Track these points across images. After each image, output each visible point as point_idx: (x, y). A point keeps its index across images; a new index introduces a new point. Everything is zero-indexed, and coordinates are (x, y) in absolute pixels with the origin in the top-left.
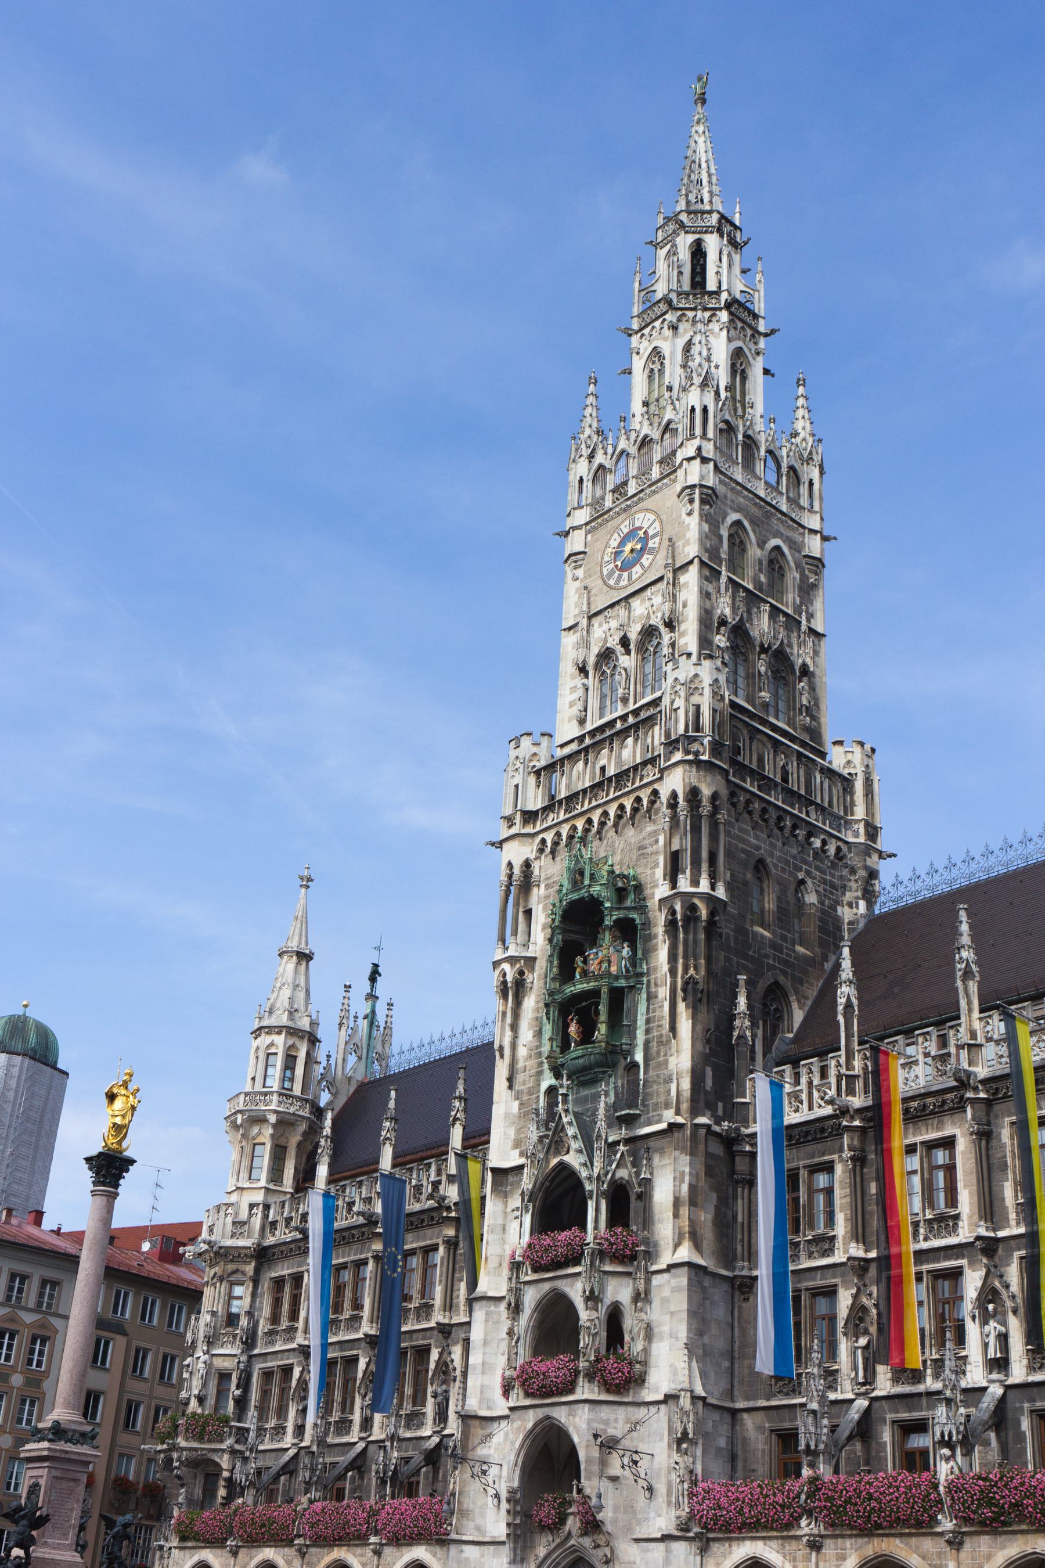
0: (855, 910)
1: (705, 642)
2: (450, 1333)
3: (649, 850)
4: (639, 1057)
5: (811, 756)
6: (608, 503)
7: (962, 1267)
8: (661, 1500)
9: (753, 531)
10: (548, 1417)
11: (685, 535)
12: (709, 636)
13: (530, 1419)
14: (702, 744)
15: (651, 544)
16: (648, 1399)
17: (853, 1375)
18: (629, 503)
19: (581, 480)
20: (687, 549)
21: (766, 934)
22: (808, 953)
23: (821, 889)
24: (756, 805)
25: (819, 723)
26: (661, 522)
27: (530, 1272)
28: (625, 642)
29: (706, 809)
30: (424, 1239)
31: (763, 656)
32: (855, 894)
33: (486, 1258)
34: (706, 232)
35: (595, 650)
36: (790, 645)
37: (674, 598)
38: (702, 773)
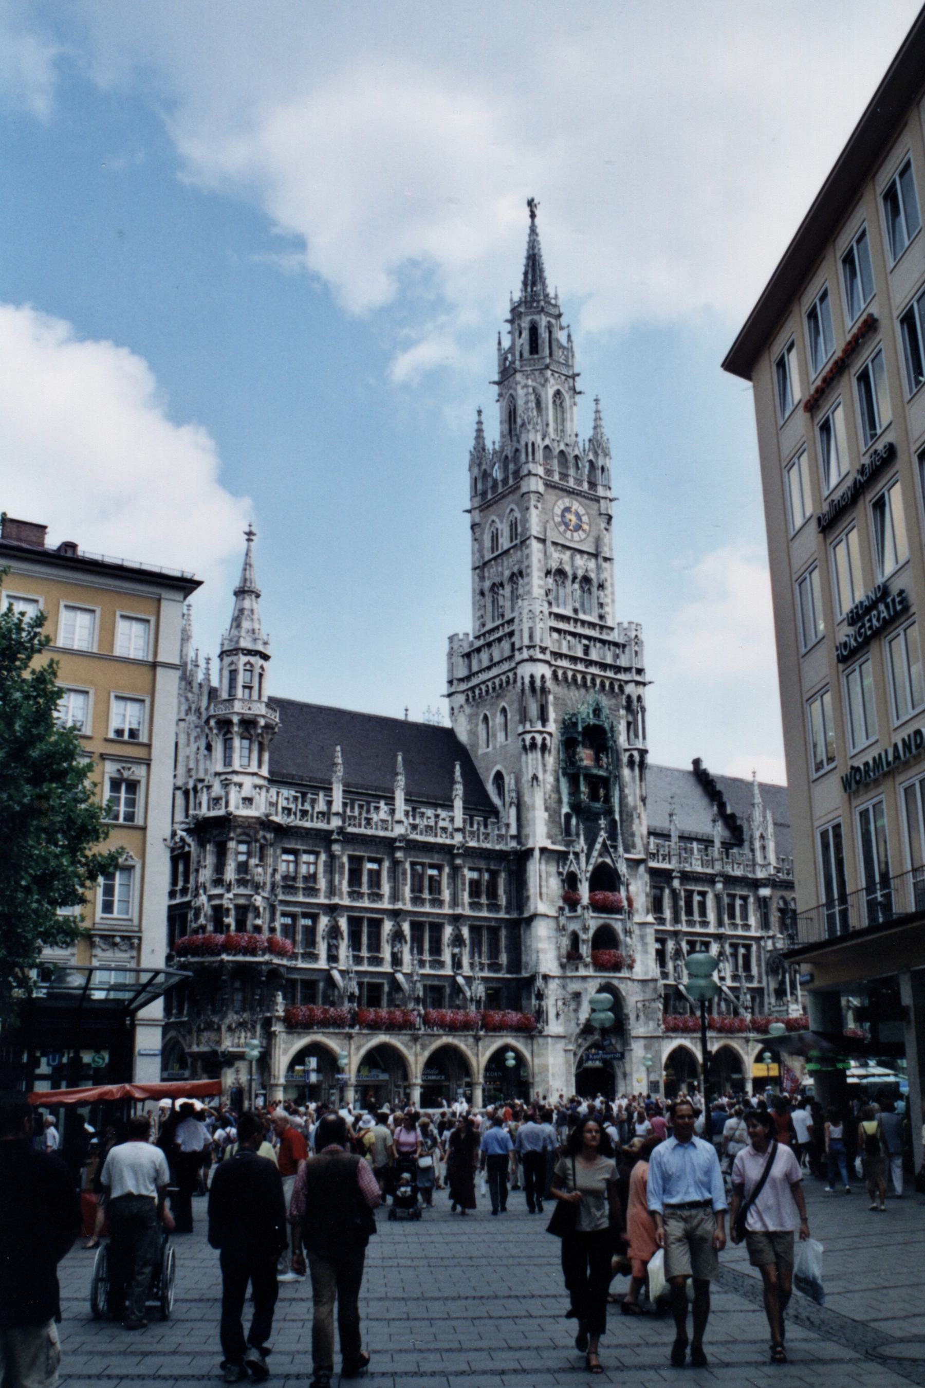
4: (617, 817)
30: (432, 858)
33: (541, 894)
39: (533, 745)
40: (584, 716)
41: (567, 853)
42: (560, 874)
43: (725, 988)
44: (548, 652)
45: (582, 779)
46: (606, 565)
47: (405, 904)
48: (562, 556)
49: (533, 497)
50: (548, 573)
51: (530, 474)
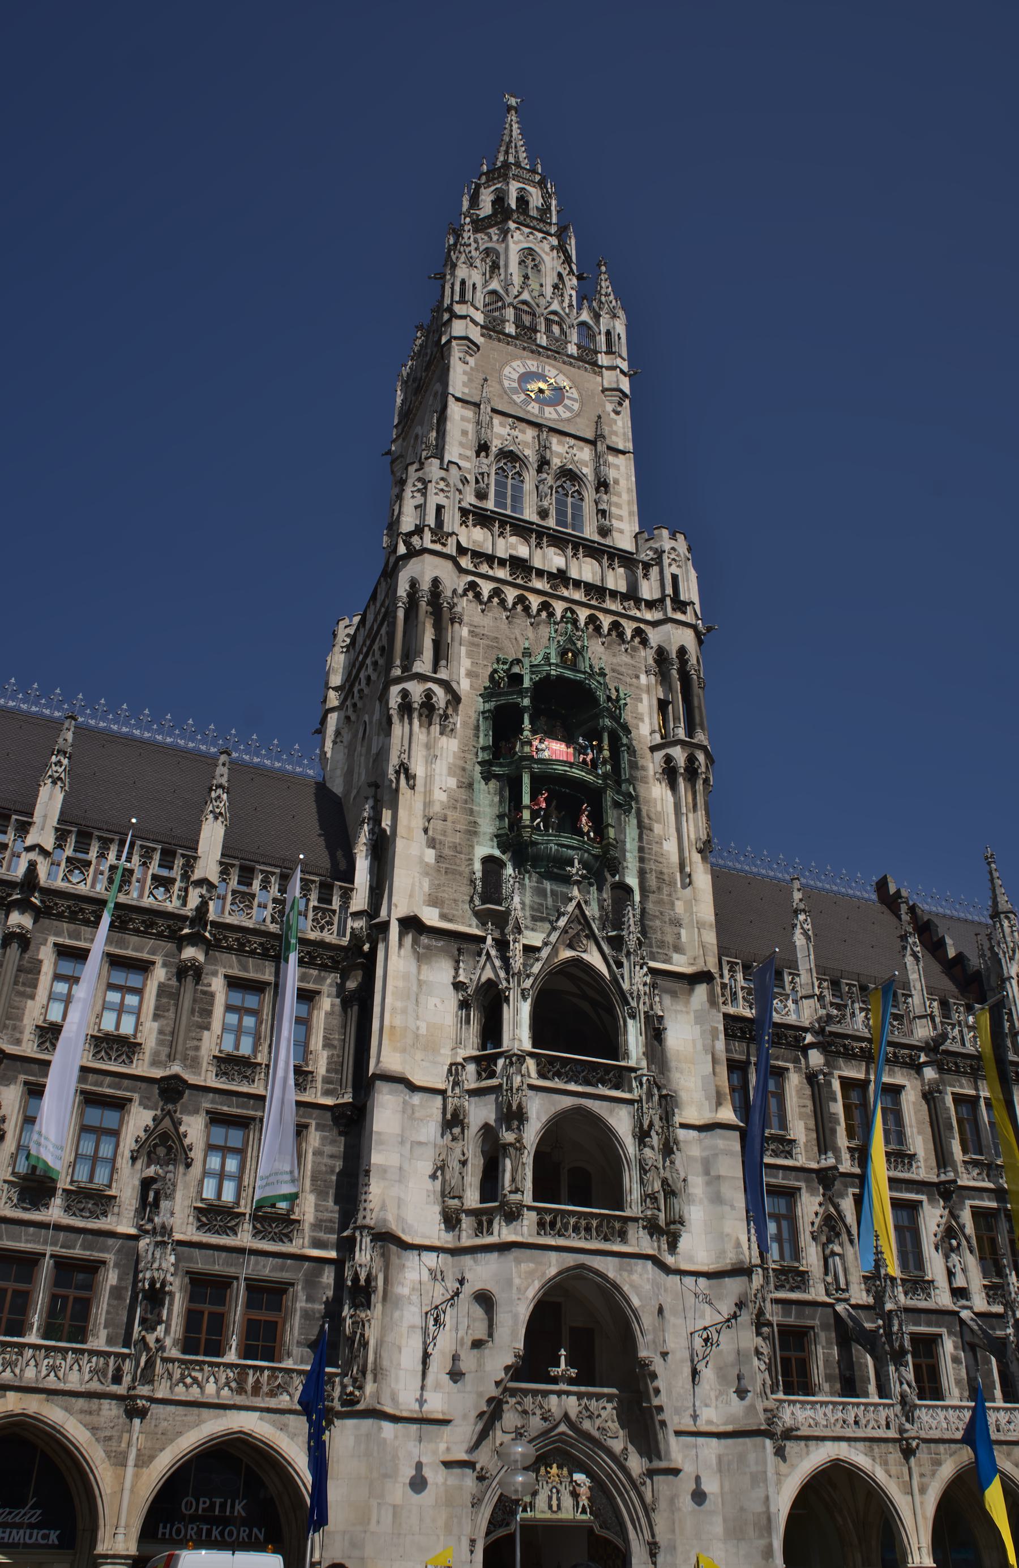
2: (181, 1094)
3: (628, 680)
4: (632, 881)
7: (921, 1202)
8: (707, 1387)
10: (582, 1266)
11: (611, 426)
13: (553, 1265)
15: (567, 401)
16: (684, 1266)
17: (829, 1279)
19: (474, 285)
20: (614, 438)
26: (580, 393)
27: (534, 1073)
39: (406, 708)
40: (538, 659)
41: (483, 940)
42: (458, 986)
43: (965, 1314)
44: (452, 542)
45: (526, 780)
46: (620, 461)
47: (18, 1042)
48: (516, 433)
49: (457, 351)
50: (483, 448)
51: (454, 316)
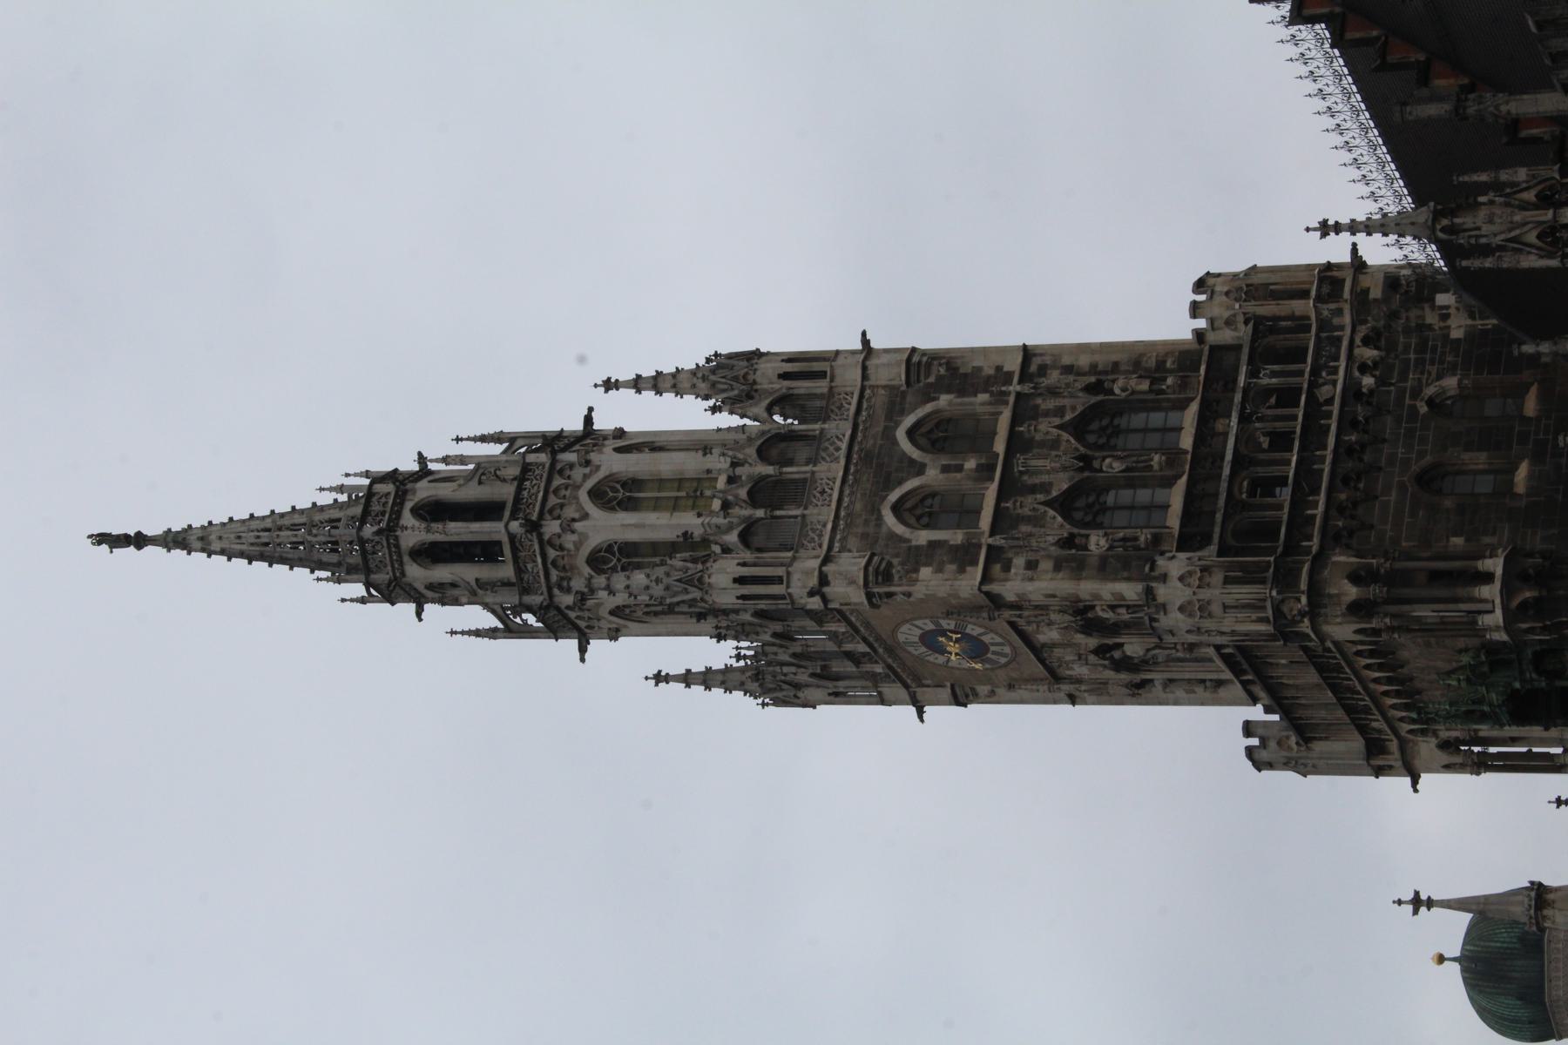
0: (1452, 311)
1: (1105, 569)
5: (1238, 397)
6: (879, 669)
9: (900, 483)
12: (1094, 561)
14: (1283, 601)
18: (881, 651)
21: (1523, 472)
22: (1533, 391)
23: (1434, 370)
24: (1343, 496)
25: (1167, 354)
28: (1101, 651)
29: (1374, 591)
31: (1096, 464)
32: (1427, 310)
34: (397, 546)
35: (1109, 674)
36: (1060, 411)
37: (1043, 608)
38: (1326, 601)
